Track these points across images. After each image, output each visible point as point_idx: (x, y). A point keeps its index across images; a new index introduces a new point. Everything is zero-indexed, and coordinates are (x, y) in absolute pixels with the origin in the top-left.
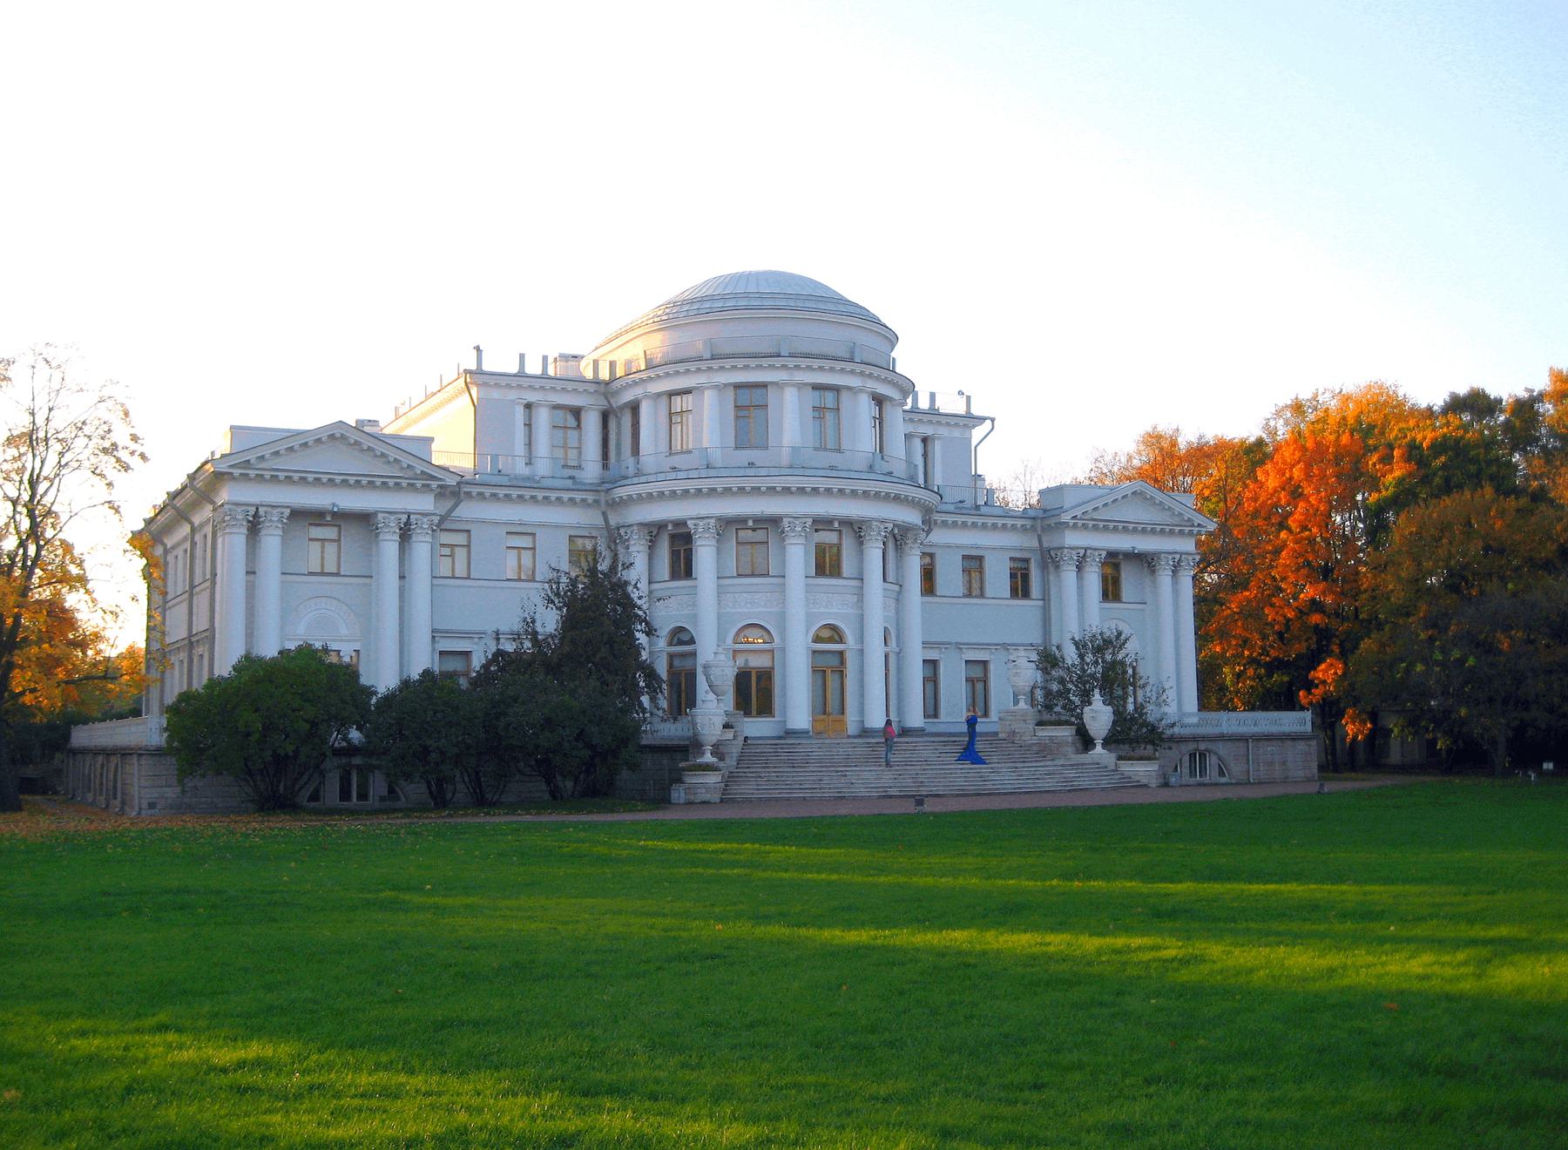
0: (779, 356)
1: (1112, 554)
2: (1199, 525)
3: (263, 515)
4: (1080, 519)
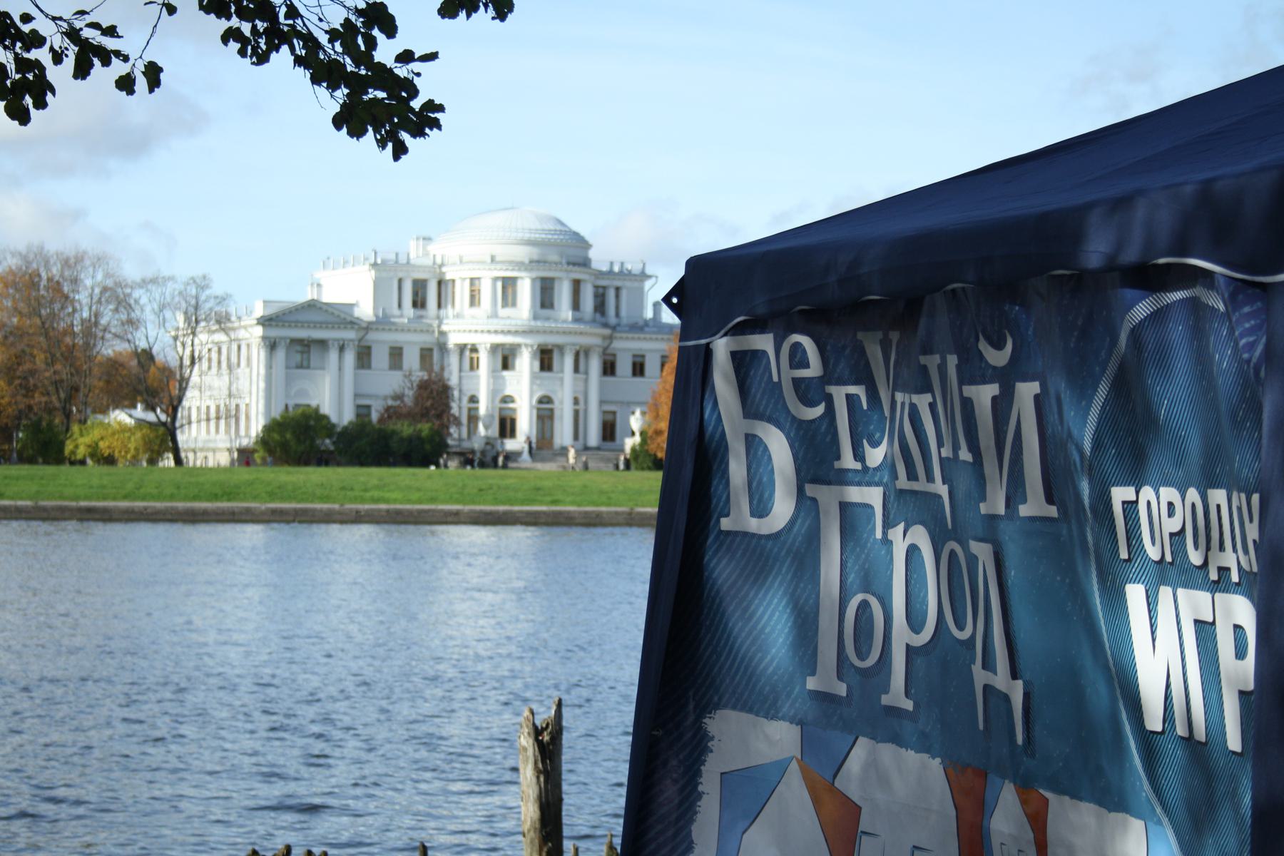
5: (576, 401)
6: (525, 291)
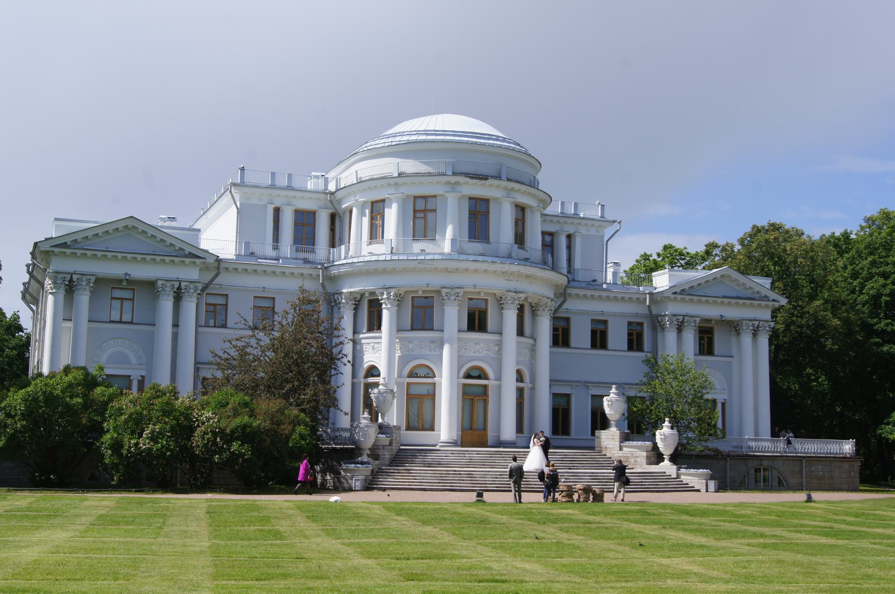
0: (445, 175)
2: (774, 300)
3: (76, 280)
4: (680, 294)
5: (520, 377)
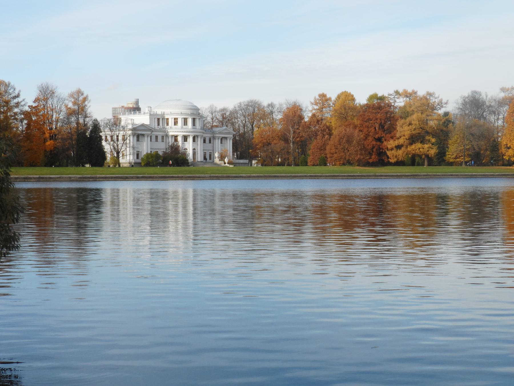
1: (222, 137)
6: (190, 121)
